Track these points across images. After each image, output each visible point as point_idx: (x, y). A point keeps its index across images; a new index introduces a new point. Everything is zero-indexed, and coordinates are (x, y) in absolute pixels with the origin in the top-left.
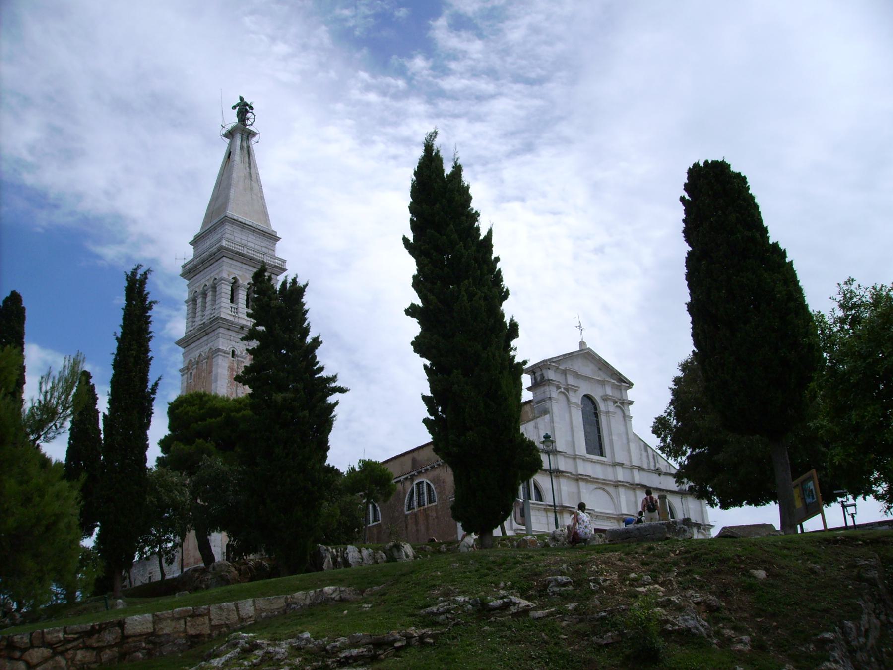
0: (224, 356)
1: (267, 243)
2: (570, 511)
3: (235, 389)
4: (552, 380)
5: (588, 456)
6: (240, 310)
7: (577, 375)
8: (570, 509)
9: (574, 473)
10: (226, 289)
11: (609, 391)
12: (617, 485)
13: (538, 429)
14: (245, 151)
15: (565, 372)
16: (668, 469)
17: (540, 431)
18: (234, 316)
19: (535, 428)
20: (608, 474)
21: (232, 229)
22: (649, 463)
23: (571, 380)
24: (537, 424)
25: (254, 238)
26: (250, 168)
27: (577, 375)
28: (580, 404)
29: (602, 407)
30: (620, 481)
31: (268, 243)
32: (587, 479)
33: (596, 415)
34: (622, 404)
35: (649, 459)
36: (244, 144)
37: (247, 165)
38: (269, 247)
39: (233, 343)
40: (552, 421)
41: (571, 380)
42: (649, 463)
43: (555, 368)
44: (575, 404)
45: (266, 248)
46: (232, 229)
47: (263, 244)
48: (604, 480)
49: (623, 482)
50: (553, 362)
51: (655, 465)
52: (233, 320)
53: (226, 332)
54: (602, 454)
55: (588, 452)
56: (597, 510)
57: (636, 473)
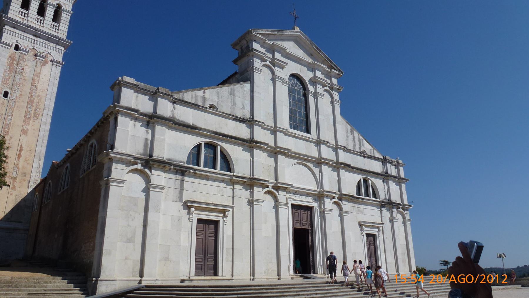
0: (5, 48)
2: (263, 184)
3: (13, 74)
4: (256, 50)
5: (292, 130)
6: (30, 15)
8: (262, 182)
9: (272, 144)
12: (319, 162)
13: (234, 95)
15: (272, 50)
16: (372, 152)
17: (237, 98)
18: (22, 19)
19: (231, 94)
20: (312, 151)
22: (354, 146)
23: (278, 56)
24: (234, 90)
28: (287, 80)
30: (323, 159)
32: (287, 153)
33: (305, 96)
34: (332, 88)
35: (355, 142)
39: (18, 39)
40: (252, 90)
42: (354, 146)
43: (261, 42)
44: (281, 79)
48: (306, 156)
49: (326, 159)
50: (259, 34)
51: (360, 148)
52: (22, 21)
53: (11, 29)
54: (308, 131)
55: (292, 126)
56: (294, 185)
57: (341, 152)
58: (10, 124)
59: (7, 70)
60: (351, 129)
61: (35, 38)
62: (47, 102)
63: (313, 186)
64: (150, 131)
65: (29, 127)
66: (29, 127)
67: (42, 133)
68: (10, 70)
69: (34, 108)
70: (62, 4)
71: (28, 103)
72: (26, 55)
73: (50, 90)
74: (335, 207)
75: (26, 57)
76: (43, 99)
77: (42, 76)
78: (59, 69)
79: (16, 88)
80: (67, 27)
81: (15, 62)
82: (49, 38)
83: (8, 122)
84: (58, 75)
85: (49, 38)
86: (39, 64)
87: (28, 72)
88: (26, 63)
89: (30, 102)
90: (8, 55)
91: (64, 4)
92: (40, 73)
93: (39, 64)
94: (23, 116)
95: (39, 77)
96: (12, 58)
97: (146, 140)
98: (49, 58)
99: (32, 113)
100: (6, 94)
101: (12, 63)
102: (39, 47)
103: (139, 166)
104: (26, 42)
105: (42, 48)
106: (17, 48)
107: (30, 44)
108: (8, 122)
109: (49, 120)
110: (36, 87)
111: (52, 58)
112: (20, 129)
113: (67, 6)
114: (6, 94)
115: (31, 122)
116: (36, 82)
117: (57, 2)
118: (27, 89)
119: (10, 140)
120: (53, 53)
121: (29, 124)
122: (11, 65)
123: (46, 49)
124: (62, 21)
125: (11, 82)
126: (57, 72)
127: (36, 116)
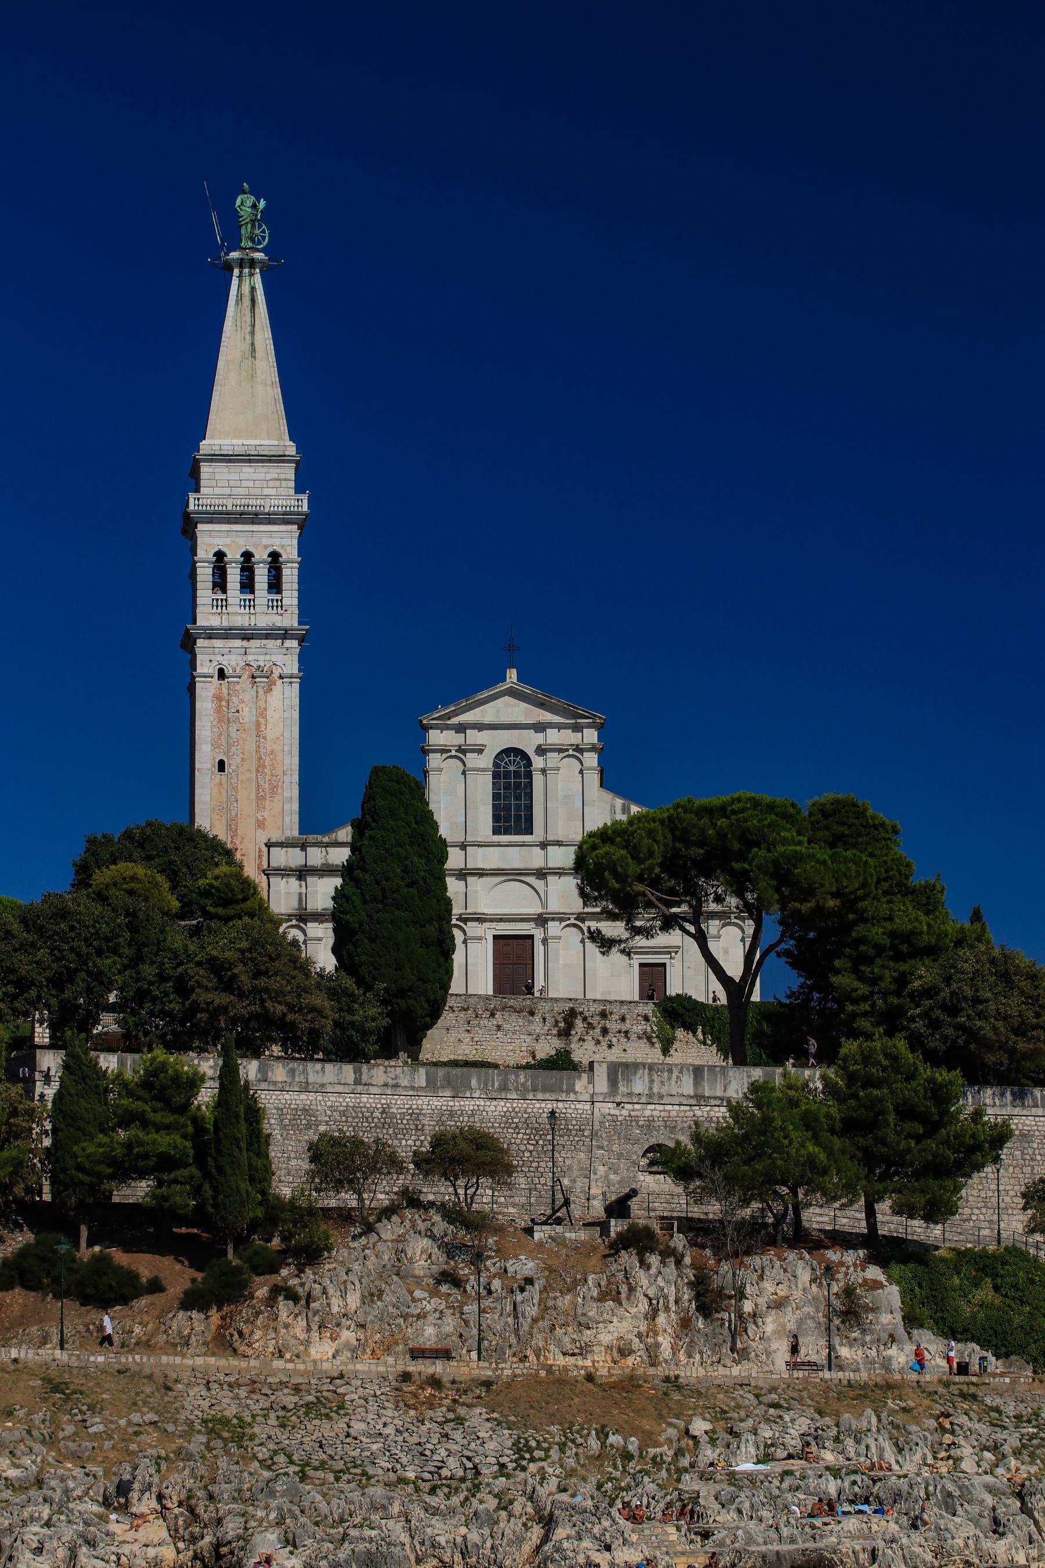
1: (278, 471)
3: (225, 727)
7: (480, 727)
10: (205, 573)
11: (554, 737)
12: (542, 874)
14: (247, 302)
20: (536, 859)
21: (211, 470)
25: (252, 470)
26: (253, 333)
27: (480, 727)
29: (538, 762)
31: (282, 471)
33: (529, 775)
36: (246, 289)
37: (249, 329)
38: (282, 476)
39: (220, 658)
41: (474, 737)
45: (277, 480)
46: (211, 470)
47: (269, 477)
58: (237, 815)
59: (215, 723)
60: (624, 805)
61: (245, 643)
62: (287, 761)
63: (534, 908)
64: (303, 883)
65: (266, 814)
66: (266, 814)
67: (287, 820)
68: (220, 721)
69: (268, 778)
70: (279, 550)
71: (258, 771)
72: (238, 683)
73: (287, 735)
74: (574, 930)
75: (237, 687)
76: (279, 758)
77: (270, 713)
78: (296, 687)
79: (234, 749)
80: (296, 594)
81: (224, 703)
82: (269, 634)
83: (233, 813)
84: (296, 701)
85: (269, 634)
86: (261, 691)
87: (247, 714)
88: (241, 697)
89: (260, 768)
90: (211, 694)
91: (283, 546)
92: (265, 709)
93: (261, 691)
94: (253, 796)
95: (265, 717)
96: (218, 698)
97: (300, 894)
98: (277, 672)
99: (267, 786)
100: (222, 766)
101: (220, 706)
102: (256, 657)
103: (294, 922)
104: (233, 657)
105: (261, 658)
106: (222, 674)
107: (239, 658)
108: (233, 813)
109: (296, 792)
110: (265, 738)
111: (280, 670)
112: (253, 821)
113: (289, 549)
114: (222, 766)
115: (267, 802)
116: (263, 727)
117: (270, 550)
118: (250, 746)
119: (241, 843)
120: (279, 659)
121: (264, 808)
122: (218, 710)
123: (268, 657)
124: (284, 586)
125: (224, 741)
126: (294, 695)
127: (274, 789)
